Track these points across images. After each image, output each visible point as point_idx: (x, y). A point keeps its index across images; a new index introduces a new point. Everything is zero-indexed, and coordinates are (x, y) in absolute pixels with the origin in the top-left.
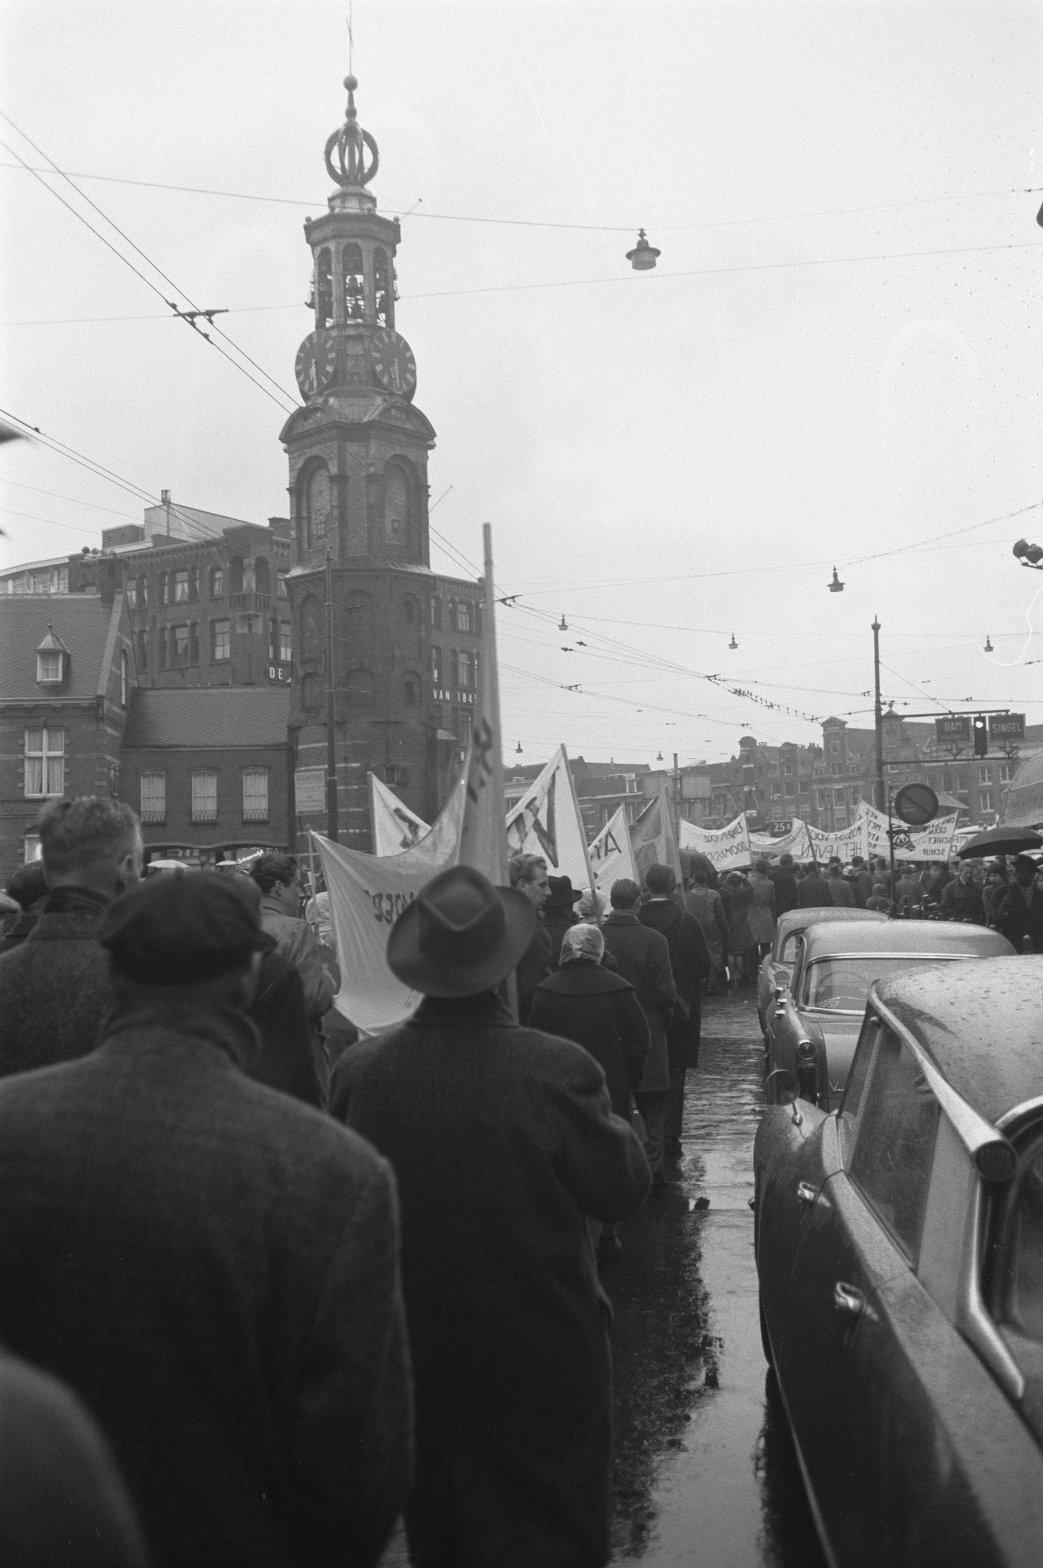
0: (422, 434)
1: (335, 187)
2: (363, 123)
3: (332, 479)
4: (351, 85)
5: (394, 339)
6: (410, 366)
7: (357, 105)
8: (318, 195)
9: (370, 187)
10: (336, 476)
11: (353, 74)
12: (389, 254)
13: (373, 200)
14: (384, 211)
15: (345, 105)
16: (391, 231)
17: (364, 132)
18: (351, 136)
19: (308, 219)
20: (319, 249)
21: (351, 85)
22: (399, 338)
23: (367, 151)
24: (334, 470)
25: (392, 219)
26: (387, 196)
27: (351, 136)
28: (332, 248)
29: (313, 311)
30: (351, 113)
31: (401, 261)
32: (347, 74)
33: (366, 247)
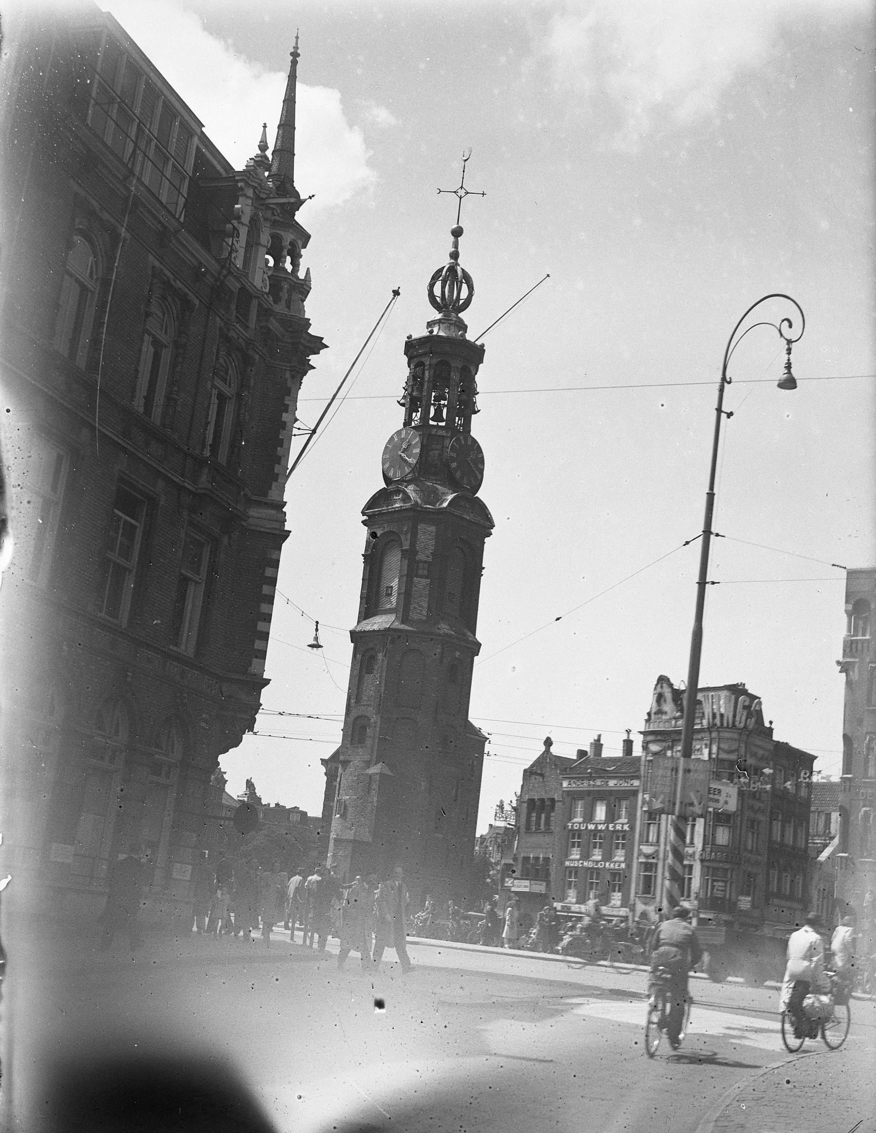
0: (483, 524)
2: (464, 263)
3: (404, 552)
4: (457, 233)
5: (469, 443)
6: (480, 466)
8: (418, 318)
10: (406, 550)
13: (464, 328)
16: (476, 354)
17: (463, 270)
20: (416, 360)
22: (474, 441)
23: (465, 287)
24: (406, 547)
26: (475, 323)
28: (427, 363)
30: (455, 255)
31: (482, 378)
33: (456, 364)
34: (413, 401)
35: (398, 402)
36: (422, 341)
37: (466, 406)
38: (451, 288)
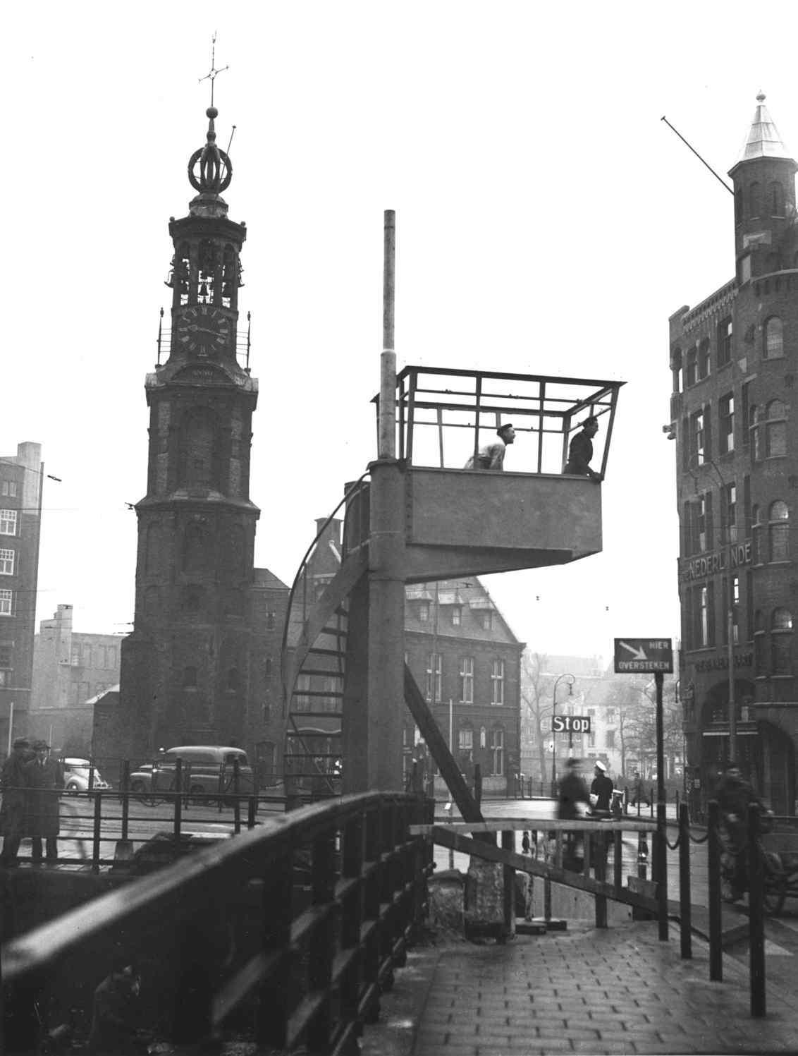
1: (197, 193)
2: (221, 144)
4: (212, 114)
7: (217, 130)
9: (224, 195)
11: (215, 106)
12: (236, 250)
13: (225, 207)
14: (233, 216)
15: (207, 129)
16: (239, 232)
18: (210, 155)
19: (172, 219)
21: (212, 114)
25: (239, 223)
26: (238, 203)
27: (210, 155)
29: (171, 290)
30: (211, 136)
31: (246, 255)
32: (209, 106)
34: (179, 281)
35: (166, 283)
36: (184, 222)
37: (231, 283)
38: (210, 169)
